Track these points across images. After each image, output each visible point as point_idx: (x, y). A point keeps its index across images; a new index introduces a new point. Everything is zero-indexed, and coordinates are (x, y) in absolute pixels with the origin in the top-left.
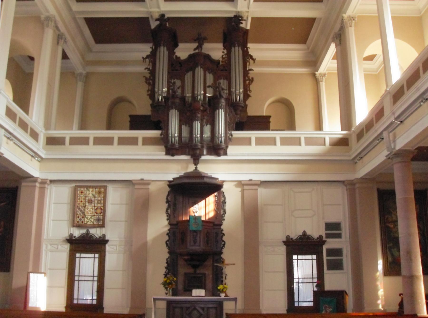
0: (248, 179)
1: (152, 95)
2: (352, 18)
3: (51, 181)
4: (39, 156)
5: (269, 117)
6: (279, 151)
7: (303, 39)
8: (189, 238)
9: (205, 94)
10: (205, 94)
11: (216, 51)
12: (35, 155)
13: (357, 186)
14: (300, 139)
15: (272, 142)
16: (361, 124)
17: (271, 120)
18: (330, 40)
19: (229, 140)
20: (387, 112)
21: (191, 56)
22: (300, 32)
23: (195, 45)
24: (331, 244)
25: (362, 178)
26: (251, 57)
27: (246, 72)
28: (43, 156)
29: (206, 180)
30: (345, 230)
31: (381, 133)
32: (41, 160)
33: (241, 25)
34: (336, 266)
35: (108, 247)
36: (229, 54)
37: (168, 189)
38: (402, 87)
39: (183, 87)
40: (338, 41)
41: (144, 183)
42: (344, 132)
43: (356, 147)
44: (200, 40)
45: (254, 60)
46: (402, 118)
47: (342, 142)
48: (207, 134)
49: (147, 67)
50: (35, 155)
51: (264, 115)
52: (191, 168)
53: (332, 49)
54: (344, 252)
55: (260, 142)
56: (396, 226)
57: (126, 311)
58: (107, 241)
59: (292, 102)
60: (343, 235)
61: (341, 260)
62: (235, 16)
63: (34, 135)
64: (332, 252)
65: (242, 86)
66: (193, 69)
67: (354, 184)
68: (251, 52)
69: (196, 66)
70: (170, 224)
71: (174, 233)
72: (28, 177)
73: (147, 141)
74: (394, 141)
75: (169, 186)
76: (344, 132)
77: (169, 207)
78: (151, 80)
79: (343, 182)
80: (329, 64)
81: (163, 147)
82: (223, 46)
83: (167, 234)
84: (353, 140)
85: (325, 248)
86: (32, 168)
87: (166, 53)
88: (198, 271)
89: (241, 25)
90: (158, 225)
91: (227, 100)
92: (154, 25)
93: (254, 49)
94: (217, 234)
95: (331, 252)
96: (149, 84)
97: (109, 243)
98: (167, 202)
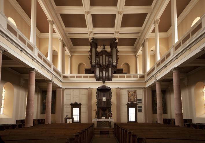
0: (117, 87)
1: (91, 63)
2: (147, 39)
3: (65, 88)
4: (62, 81)
5: (123, 69)
6: (126, 79)
7: (132, 44)
8: (103, 104)
9: (105, 63)
10: (105, 63)
11: (108, 49)
12: (61, 81)
13: (146, 89)
14: (131, 76)
15: (124, 77)
16: (148, 72)
17: (123, 70)
18: (141, 45)
19: (113, 76)
20: (155, 69)
21: (102, 51)
22: (131, 42)
23: (103, 47)
24: (139, 105)
25: (148, 87)
26: (118, 51)
27: (117, 56)
28: (63, 81)
29: (107, 88)
30: (143, 101)
31: (153, 75)
32: (62, 82)
33: (116, 41)
34: (140, 111)
35: (81, 106)
36: (112, 50)
37: (97, 90)
38: (160, 62)
39: (99, 62)
40: (143, 46)
41: (90, 89)
42: (143, 74)
43: (146, 78)
44: (104, 46)
45: (119, 52)
46: (159, 71)
47: (143, 77)
48: (107, 75)
49: (89, 54)
50: (61, 81)
51: (121, 68)
52: (103, 84)
53: (141, 48)
54: (142, 107)
55: (121, 77)
56: (156, 100)
57: (87, 123)
58: (81, 104)
59: (129, 64)
60: (142, 103)
61: (142, 109)
62: (114, 38)
63: (60, 76)
64: (139, 107)
65: (116, 60)
66: (102, 55)
67: (145, 89)
68: (118, 50)
69: (103, 54)
70: (97, 100)
71: (99, 102)
72: (59, 87)
73: (91, 77)
74: (157, 77)
75: (97, 89)
76: (143, 74)
77: (97, 95)
78: (90, 58)
79: (142, 88)
80: (140, 52)
81: (95, 79)
82: (110, 47)
83: (97, 102)
84: (146, 76)
85: (137, 106)
86: (60, 85)
87: (95, 50)
88: (105, 112)
89: (116, 41)
90: (94, 100)
91: (112, 65)
92: (91, 41)
93: (120, 48)
94: (109, 102)
95: (139, 107)
96: (90, 60)
97: (82, 105)
98: (97, 94)
